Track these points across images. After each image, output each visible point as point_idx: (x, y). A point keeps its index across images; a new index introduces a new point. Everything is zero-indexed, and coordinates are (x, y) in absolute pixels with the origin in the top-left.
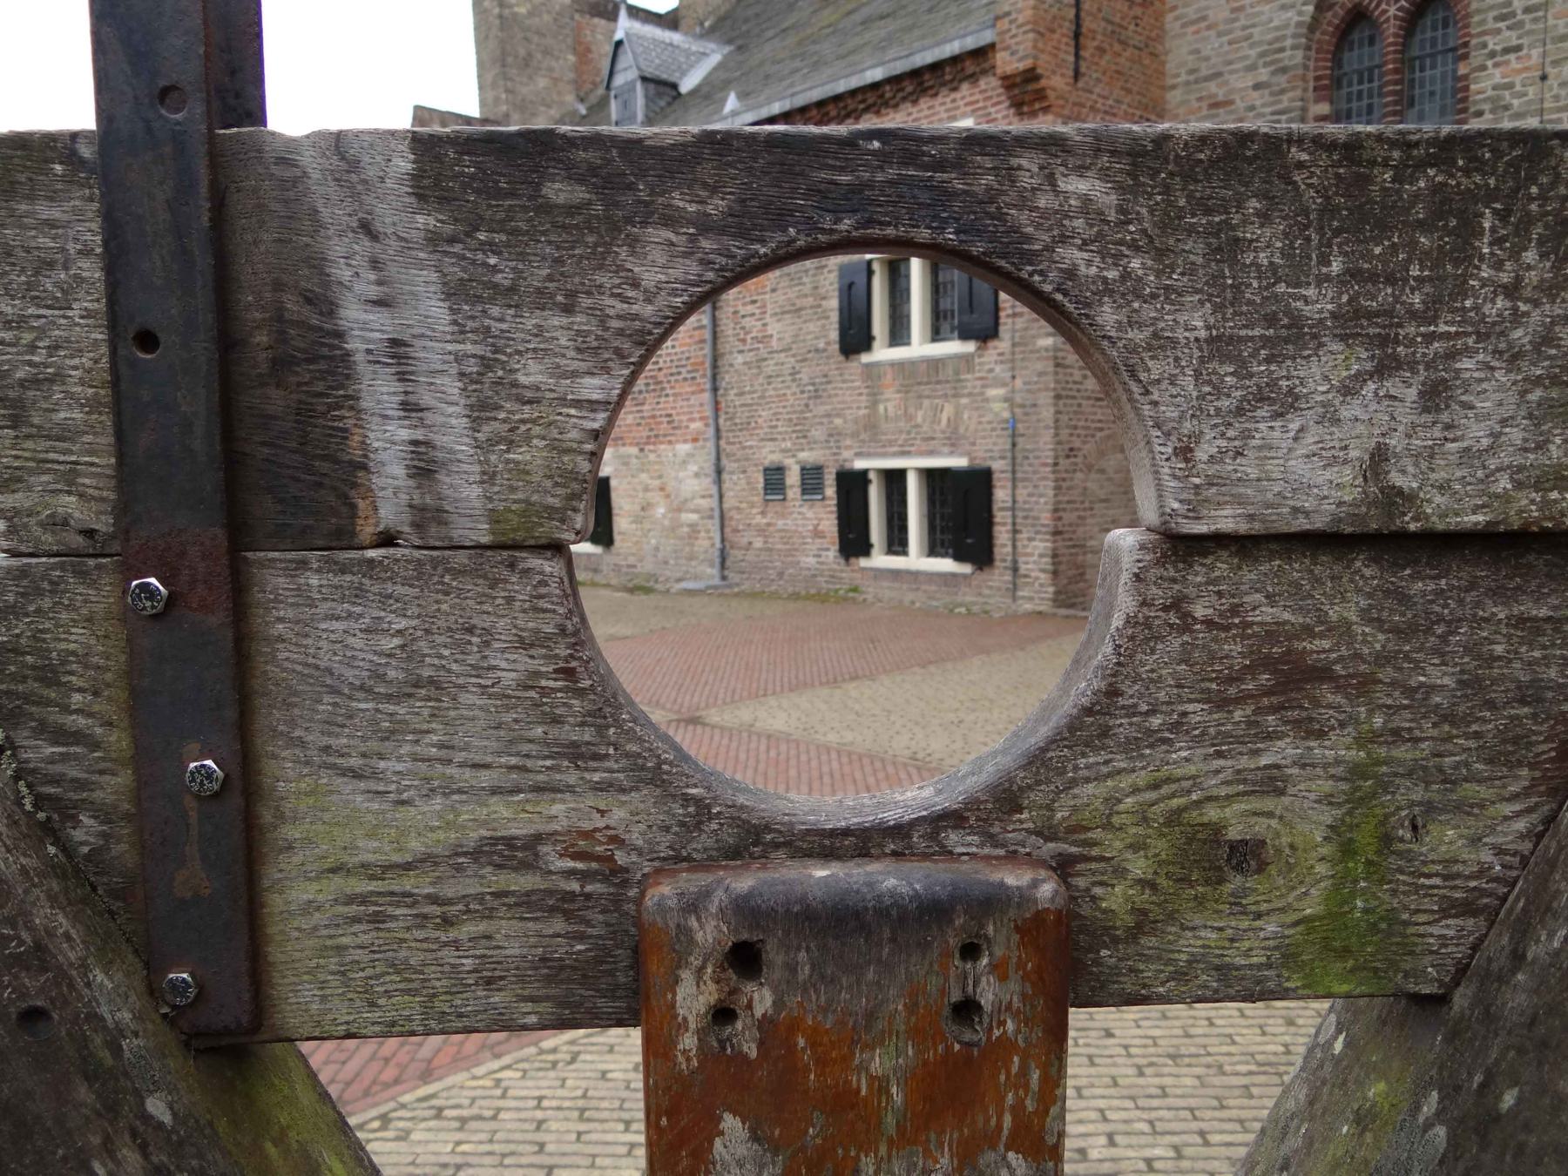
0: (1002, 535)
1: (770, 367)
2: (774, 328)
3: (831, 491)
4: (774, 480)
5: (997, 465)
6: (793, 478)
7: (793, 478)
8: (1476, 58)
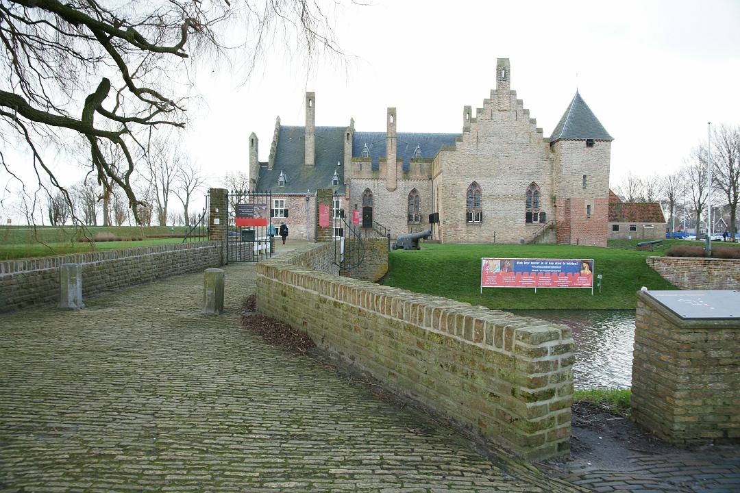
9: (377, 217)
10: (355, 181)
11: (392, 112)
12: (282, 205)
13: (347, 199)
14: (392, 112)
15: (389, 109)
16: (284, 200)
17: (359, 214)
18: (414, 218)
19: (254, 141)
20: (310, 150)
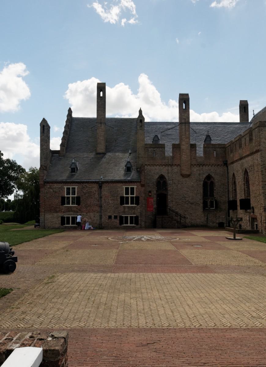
0: (140, 222)
1: (110, 205)
2: (110, 202)
3: (118, 218)
4: (110, 217)
5: (139, 216)
6: (113, 217)
7: (113, 217)
8: (168, 187)
9: (171, 204)
10: (149, 167)
11: (184, 100)
12: (74, 193)
13: (143, 186)
14: (184, 100)
15: (181, 95)
16: (76, 187)
17: (153, 201)
18: (209, 203)
19: (45, 127)
20: (102, 138)
